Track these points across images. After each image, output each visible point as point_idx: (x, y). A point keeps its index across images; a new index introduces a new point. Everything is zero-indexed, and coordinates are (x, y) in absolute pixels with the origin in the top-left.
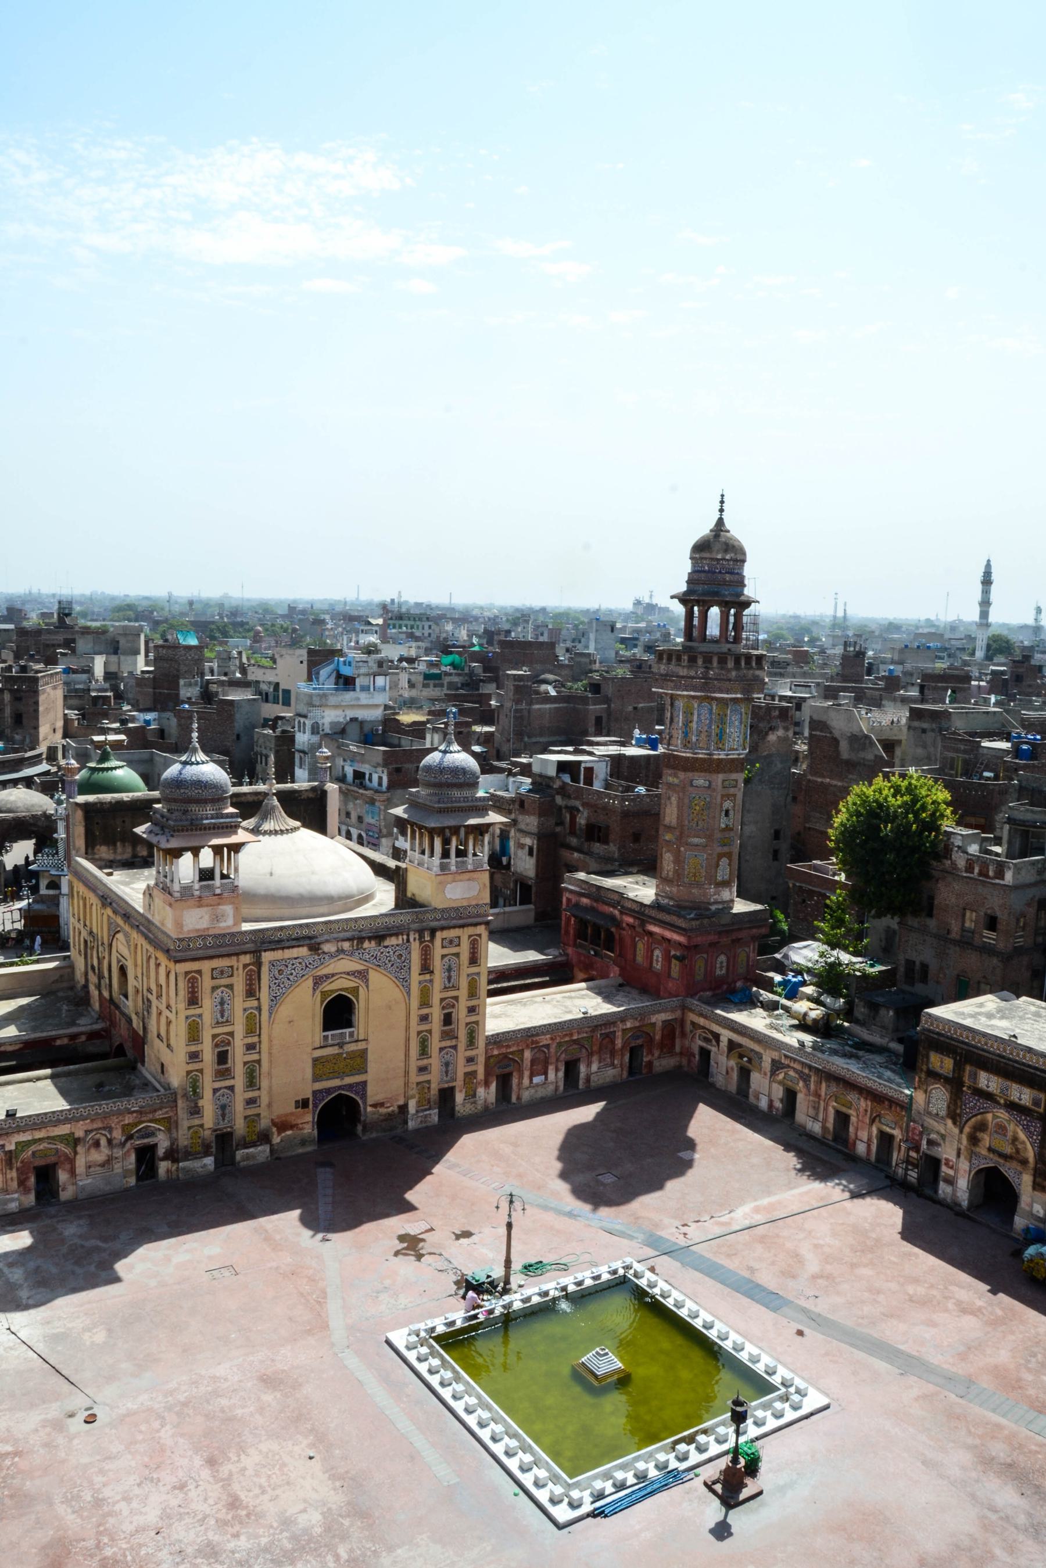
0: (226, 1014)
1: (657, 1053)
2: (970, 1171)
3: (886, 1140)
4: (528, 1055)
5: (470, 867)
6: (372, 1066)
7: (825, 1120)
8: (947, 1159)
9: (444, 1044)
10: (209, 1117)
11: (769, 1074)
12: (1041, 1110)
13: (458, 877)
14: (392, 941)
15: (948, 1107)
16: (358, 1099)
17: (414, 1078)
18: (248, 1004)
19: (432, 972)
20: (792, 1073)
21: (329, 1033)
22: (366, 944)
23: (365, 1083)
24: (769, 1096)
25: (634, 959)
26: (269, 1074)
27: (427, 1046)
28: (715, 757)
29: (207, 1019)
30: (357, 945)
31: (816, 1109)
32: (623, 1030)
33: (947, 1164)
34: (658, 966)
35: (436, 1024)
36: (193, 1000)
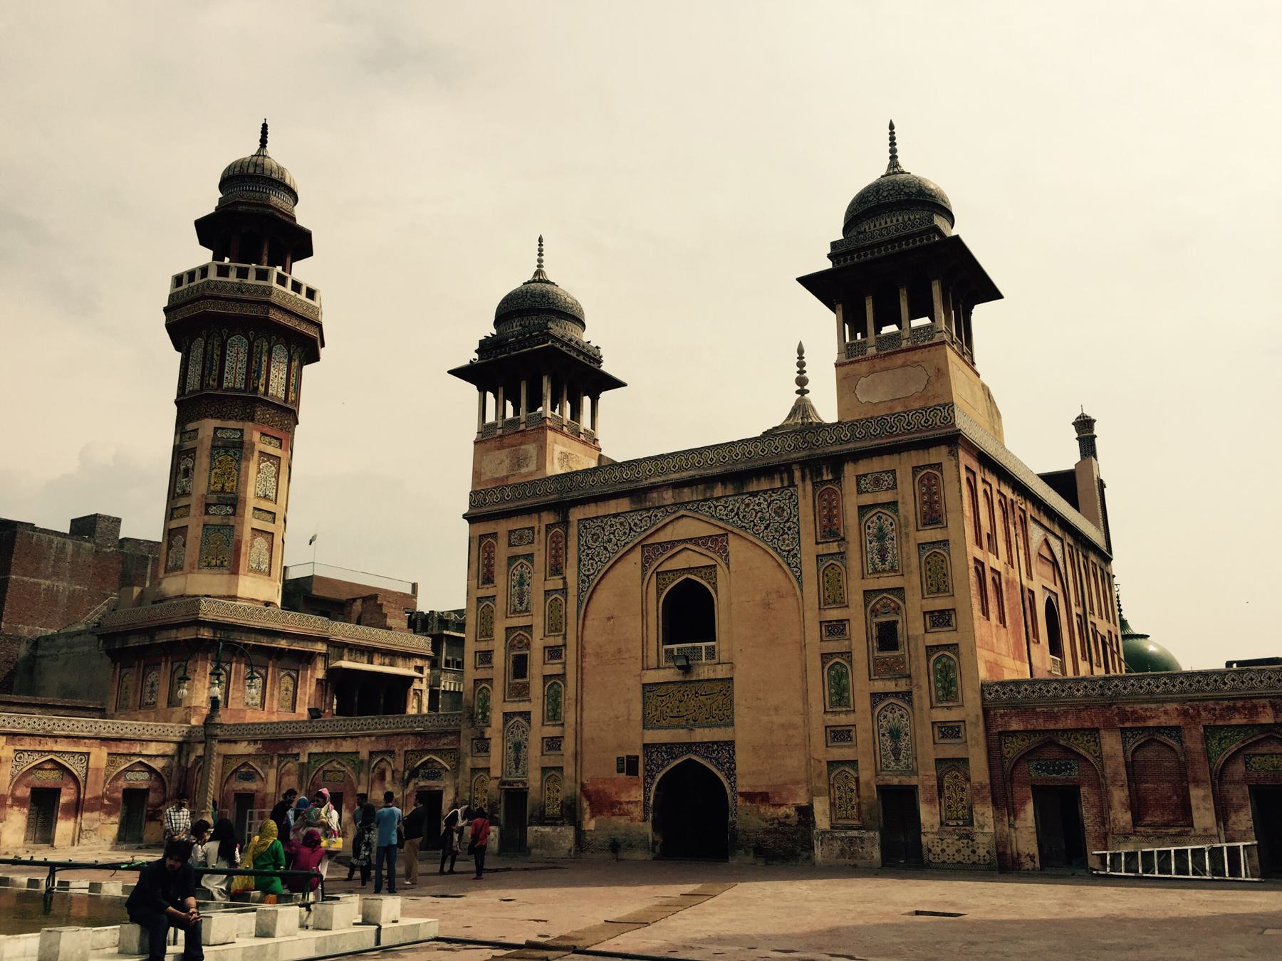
0: (525, 602)
4: (1111, 744)
5: (904, 344)
6: (742, 714)
9: (879, 686)
10: (496, 759)
13: (880, 364)
14: (764, 485)
16: (721, 776)
17: (824, 752)
18: (550, 585)
19: (843, 539)
21: (675, 646)
22: (719, 491)
23: (731, 744)
26: (579, 702)
27: (845, 689)
29: (500, 606)
30: (705, 490)
35: (859, 638)
36: (488, 579)
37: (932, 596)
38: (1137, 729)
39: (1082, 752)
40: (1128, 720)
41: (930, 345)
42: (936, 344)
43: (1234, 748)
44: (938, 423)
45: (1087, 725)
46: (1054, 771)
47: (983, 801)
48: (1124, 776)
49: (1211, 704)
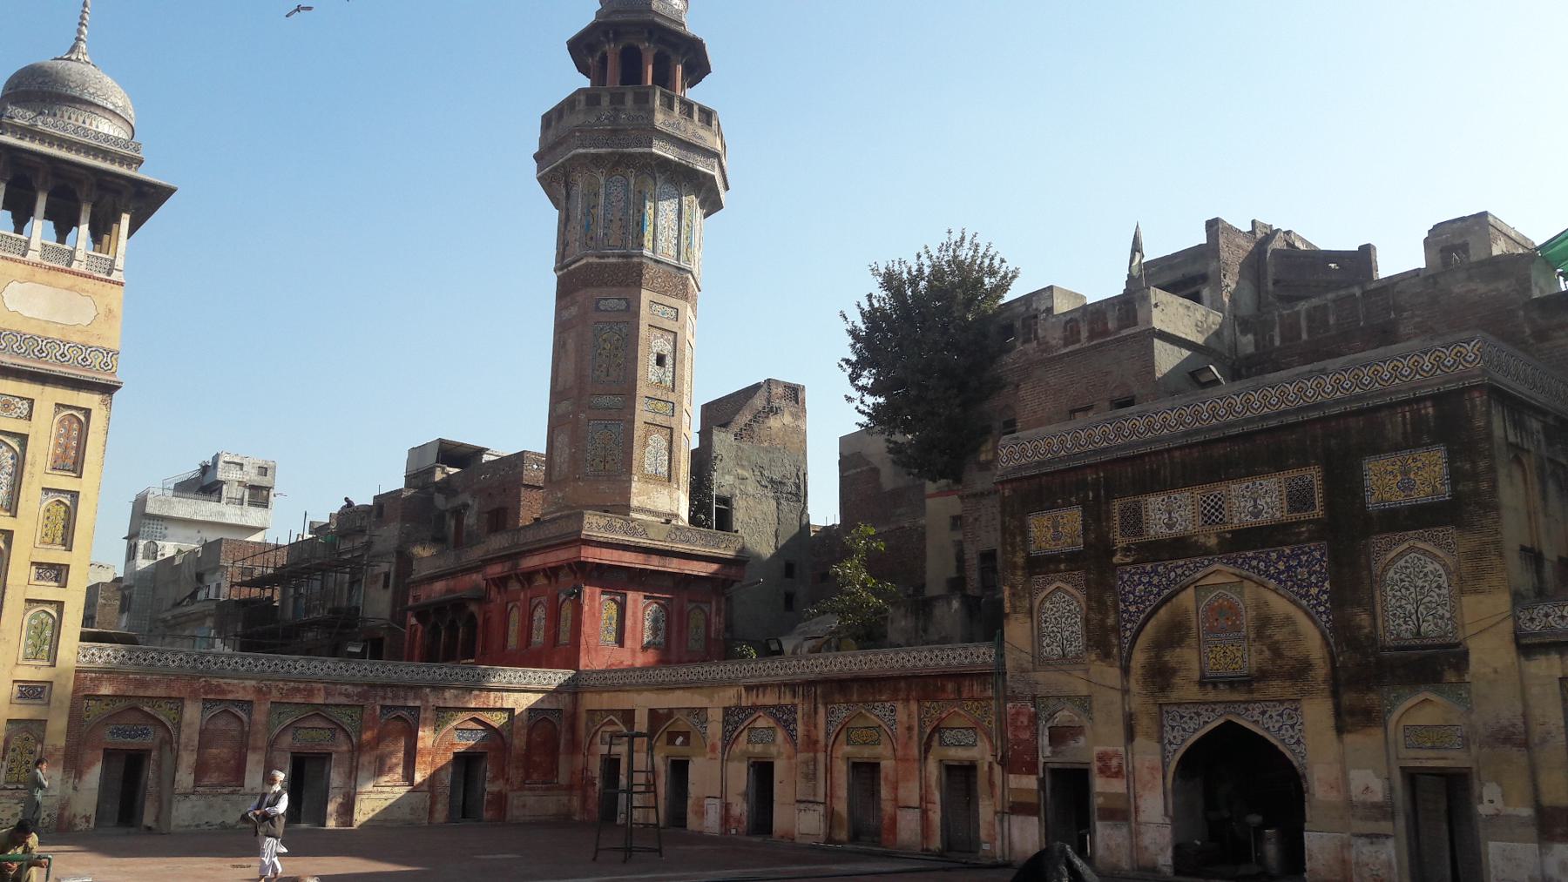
1: (515, 774)
2: (1165, 765)
3: (961, 777)
4: (193, 713)
7: (830, 794)
8: (1102, 757)
11: (719, 744)
12: (1318, 512)
13: (40, 274)
15: (1087, 621)
20: (762, 723)
24: (723, 795)
25: (505, 646)
28: (635, 260)
31: (811, 777)
32: (438, 708)
33: (1105, 771)
34: (538, 638)
37: (45, 546)
38: (215, 700)
39: (162, 718)
40: (211, 693)
41: (106, 280)
42: (114, 282)
43: (288, 722)
44: (98, 367)
45: (174, 694)
46: (129, 736)
47: (53, 765)
48: (196, 743)
49: (281, 685)
